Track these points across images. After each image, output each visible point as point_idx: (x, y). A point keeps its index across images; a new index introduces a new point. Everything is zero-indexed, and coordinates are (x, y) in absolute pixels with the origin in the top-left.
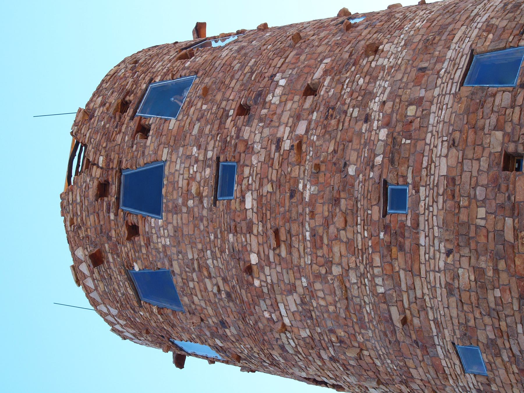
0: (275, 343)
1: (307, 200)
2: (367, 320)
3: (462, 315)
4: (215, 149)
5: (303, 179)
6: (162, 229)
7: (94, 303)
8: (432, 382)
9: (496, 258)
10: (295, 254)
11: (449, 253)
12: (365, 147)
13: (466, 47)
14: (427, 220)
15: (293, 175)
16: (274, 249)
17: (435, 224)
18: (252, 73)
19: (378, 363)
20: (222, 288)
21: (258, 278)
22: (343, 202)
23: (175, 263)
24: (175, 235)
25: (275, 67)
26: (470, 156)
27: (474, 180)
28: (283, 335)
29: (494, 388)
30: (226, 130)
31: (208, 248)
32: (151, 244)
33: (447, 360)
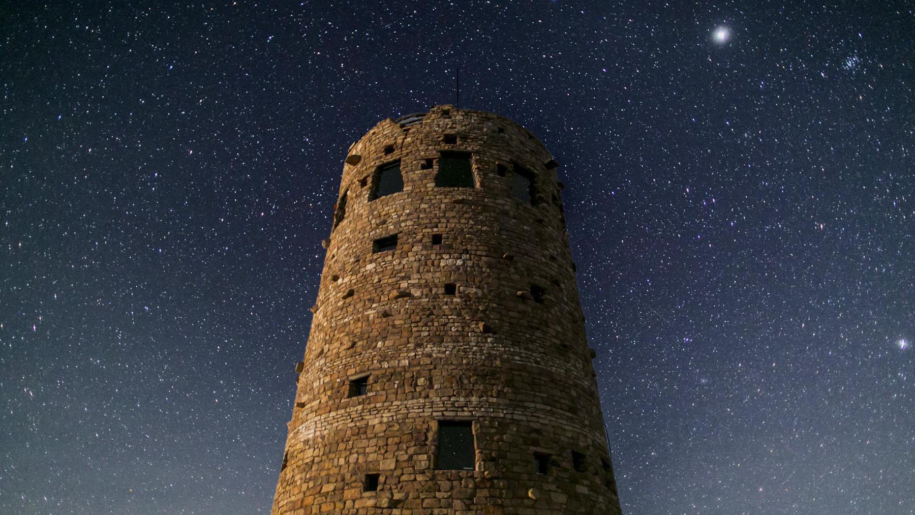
14: (342, 416)
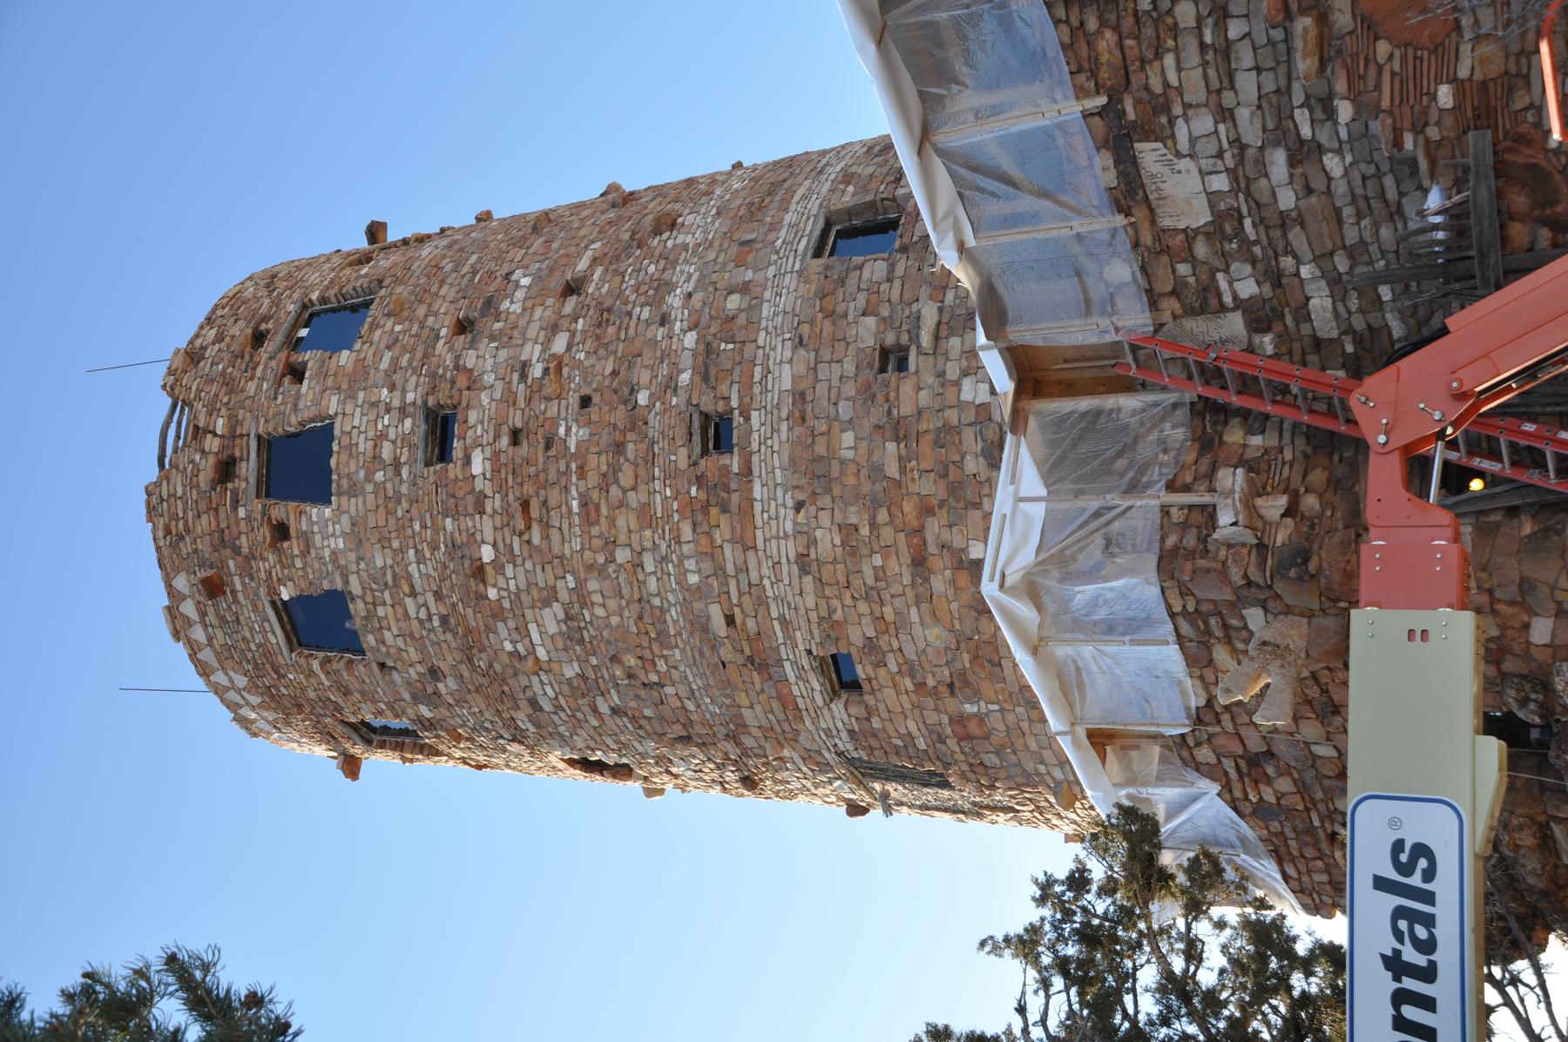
0: (521, 695)
1: (573, 450)
2: (672, 633)
3: (822, 603)
4: (419, 389)
5: (566, 419)
6: (330, 523)
7: (204, 671)
8: (778, 729)
9: (874, 504)
10: (555, 536)
11: (799, 506)
12: (662, 362)
13: (814, 206)
14: (765, 461)
15: (549, 414)
16: (521, 535)
17: (777, 464)
18: (474, 273)
19: (690, 706)
20: (433, 611)
21: (494, 586)
22: (631, 447)
23: (353, 579)
24: (353, 531)
25: (512, 261)
26: (827, 357)
27: (834, 392)
28: (535, 679)
29: (876, 723)
30: (435, 360)
31: (411, 544)
32: (312, 551)
33: (801, 683)
